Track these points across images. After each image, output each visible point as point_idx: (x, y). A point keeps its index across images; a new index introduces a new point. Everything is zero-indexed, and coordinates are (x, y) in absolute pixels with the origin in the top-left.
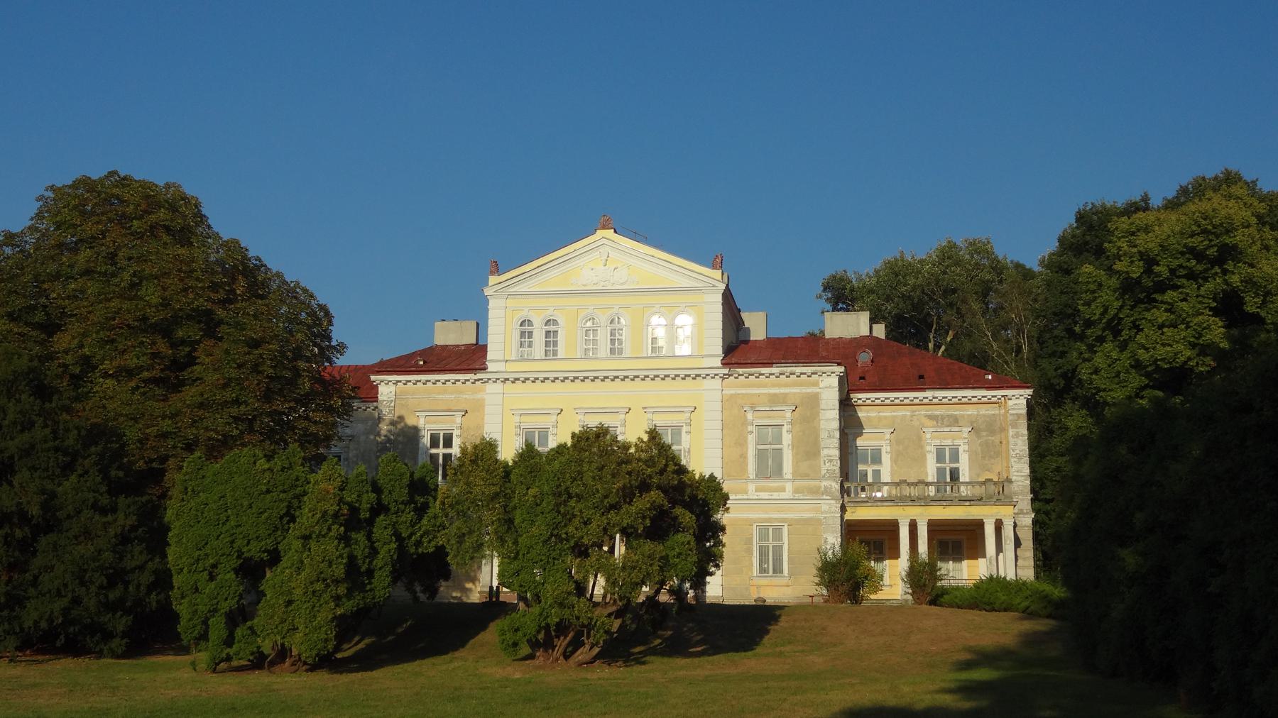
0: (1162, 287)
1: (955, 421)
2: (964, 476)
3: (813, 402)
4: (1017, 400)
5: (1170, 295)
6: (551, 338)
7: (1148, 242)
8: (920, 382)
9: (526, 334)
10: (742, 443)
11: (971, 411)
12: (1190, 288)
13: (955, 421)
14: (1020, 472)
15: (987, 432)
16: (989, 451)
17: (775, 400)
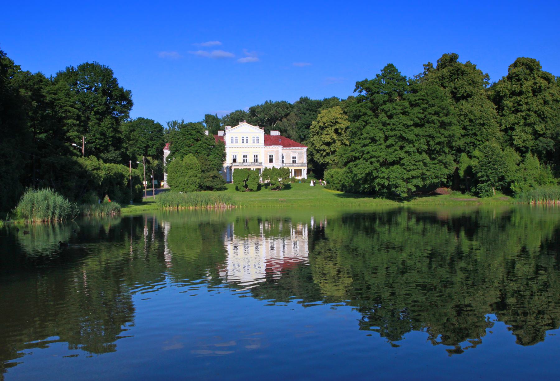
0: (326, 127)
1: (295, 152)
2: (297, 162)
3: (278, 151)
4: (305, 149)
5: (327, 129)
6: (237, 140)
7: (324, 120)
8: (289, 146)
9: (232, 140)
10: (267, 157)
11: (298, 151)
12: (330, 128)
13: (295, 152)
14: (305, 161)
15: (300, 154)
16: (301, 157)
17: (272, 151)
